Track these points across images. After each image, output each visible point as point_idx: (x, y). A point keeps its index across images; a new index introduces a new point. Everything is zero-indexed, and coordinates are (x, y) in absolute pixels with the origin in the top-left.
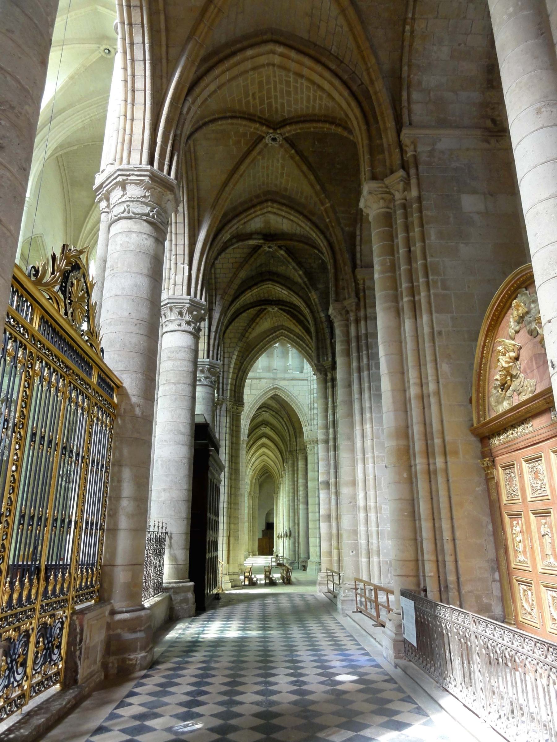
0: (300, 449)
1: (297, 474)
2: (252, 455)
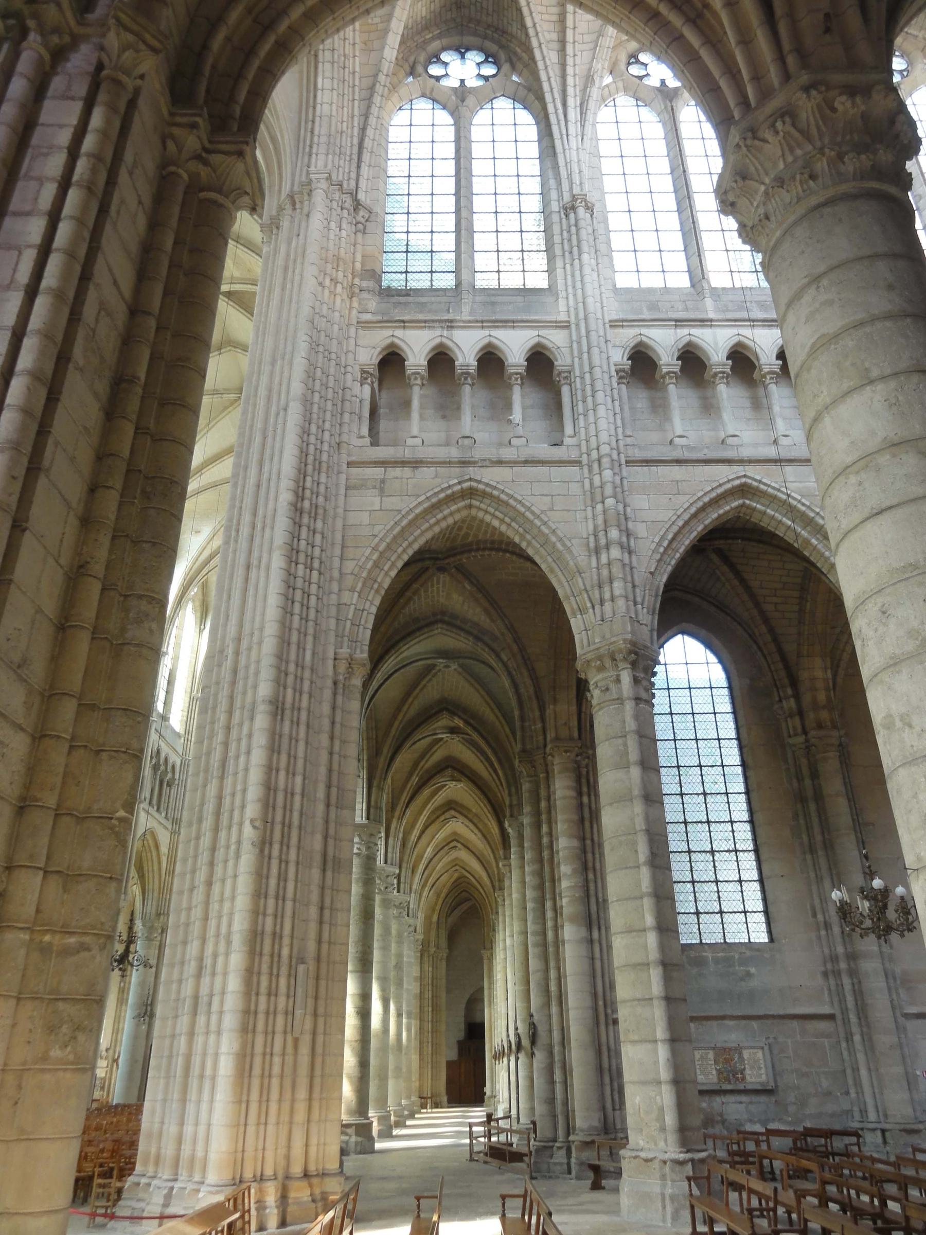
0: (557, 739)
2: (423, 832)
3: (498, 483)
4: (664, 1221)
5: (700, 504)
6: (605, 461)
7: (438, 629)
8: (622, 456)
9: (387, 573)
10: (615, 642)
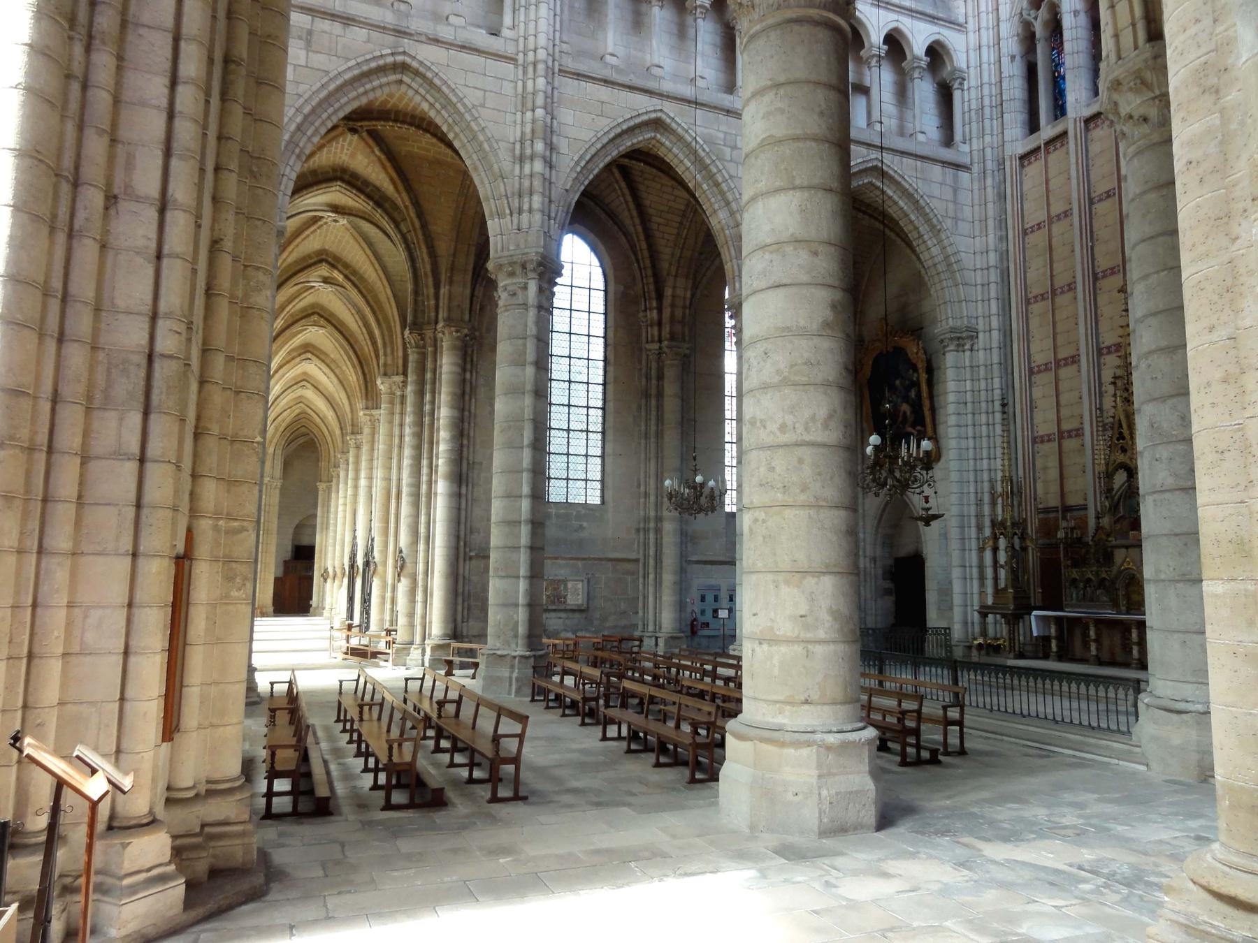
1: (433, 392)
3: (432, 63)
4: (509, 693)
5: (619, 130)
6: (541, 67)
7: (337, 186)
8: (556, 63)
9: (309, 139)
10: (527, 253)
